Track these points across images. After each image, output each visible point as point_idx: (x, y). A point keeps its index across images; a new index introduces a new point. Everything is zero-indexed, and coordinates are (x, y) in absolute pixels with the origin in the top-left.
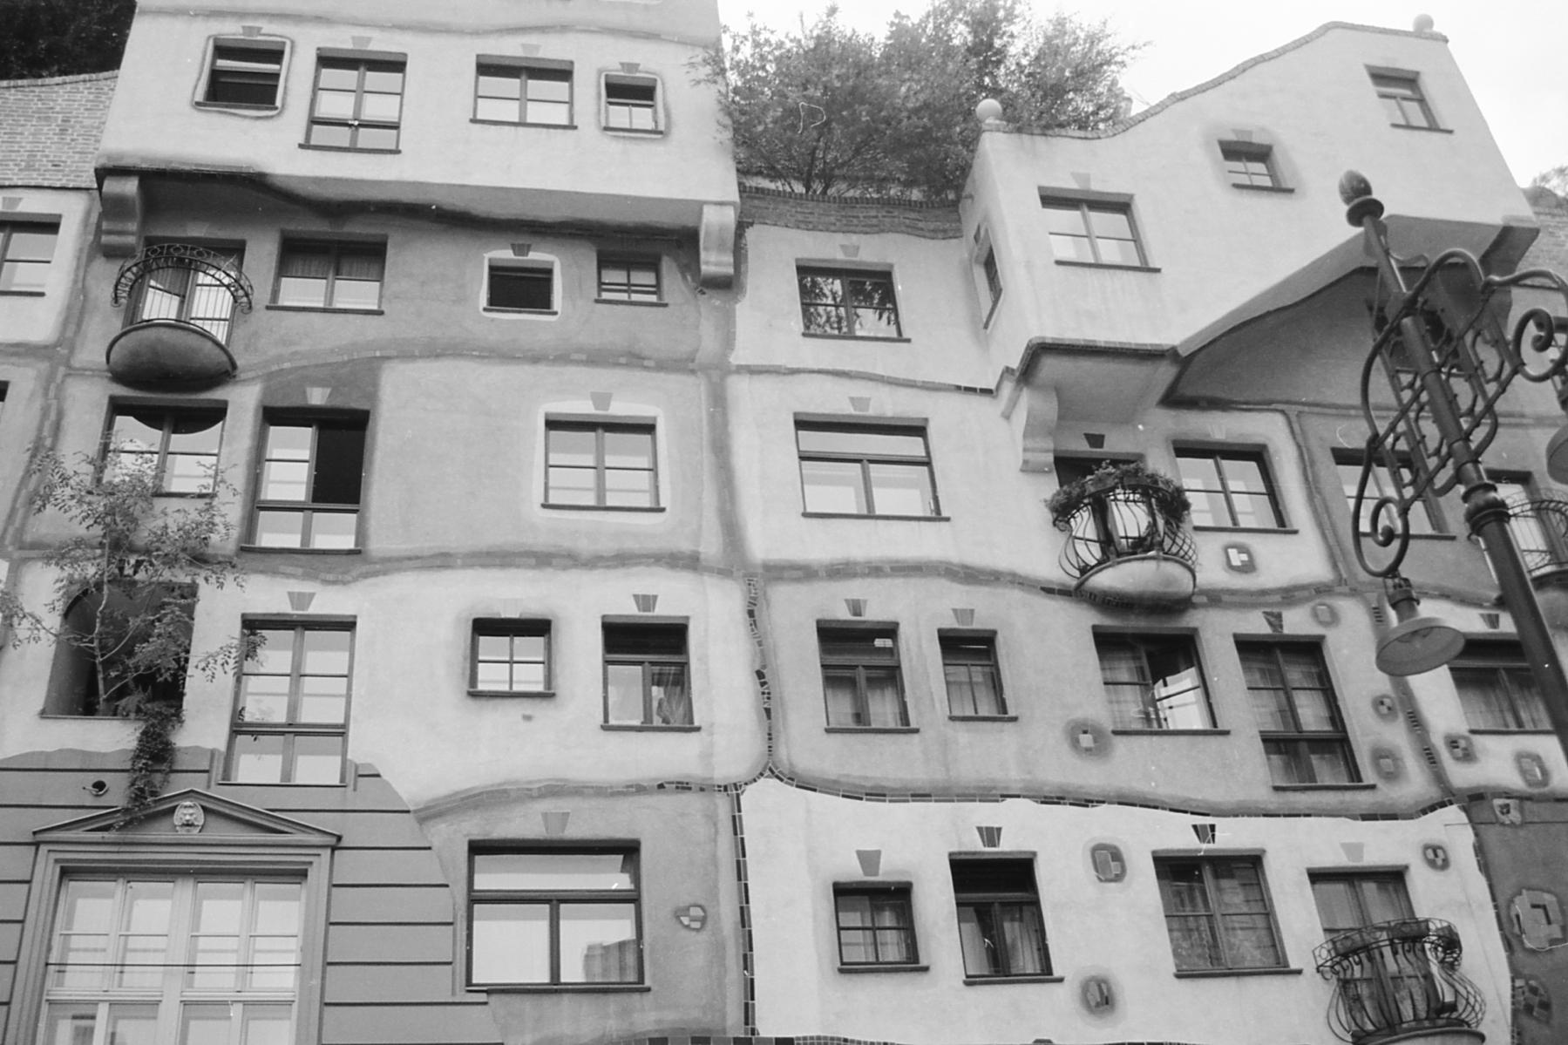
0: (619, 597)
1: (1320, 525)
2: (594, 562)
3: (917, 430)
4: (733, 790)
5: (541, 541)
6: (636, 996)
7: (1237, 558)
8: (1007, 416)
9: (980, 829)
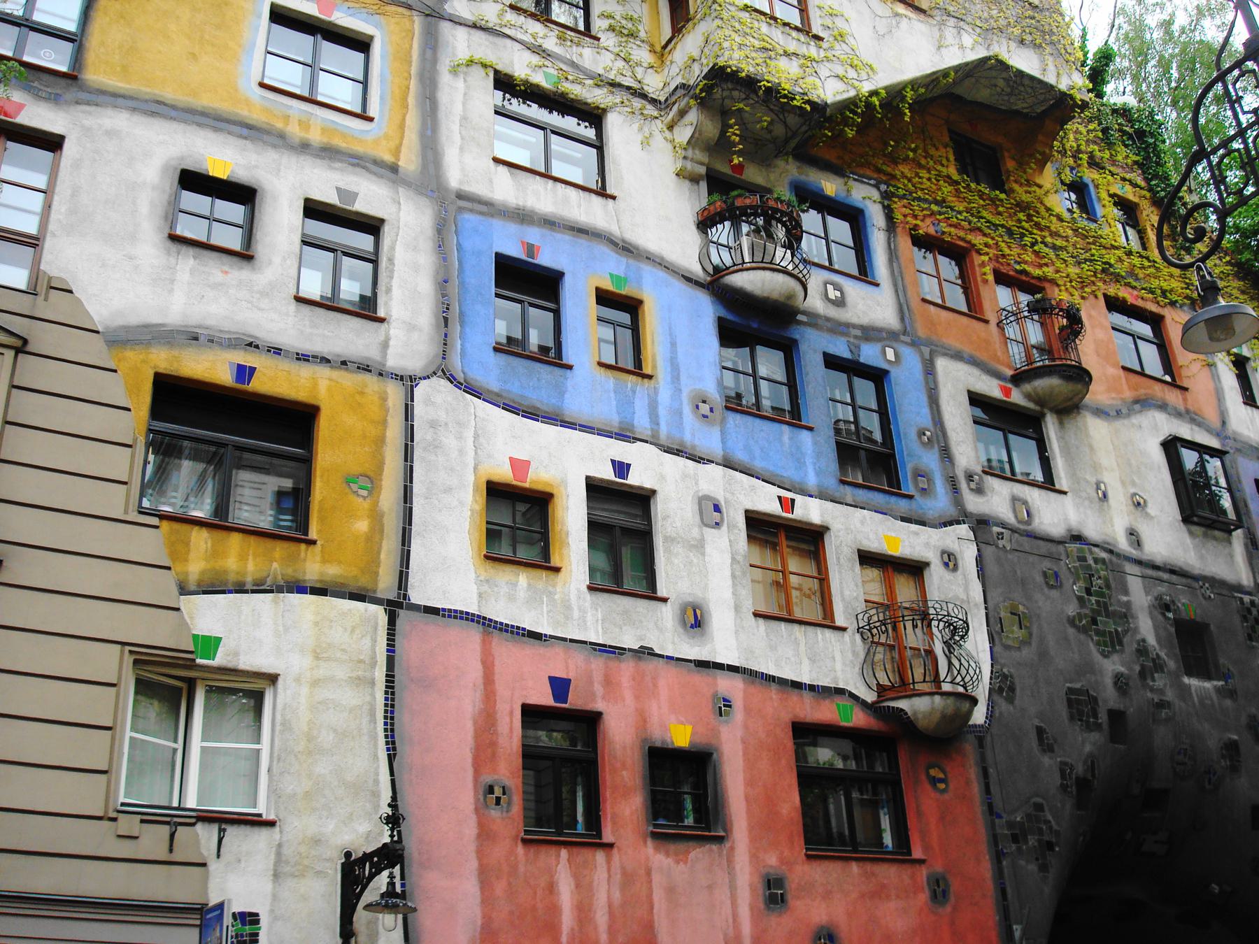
0: (326, 184)
1: (895, 285)
2: (304, 147)
3: (594, 117)
4: (409, 382)
5: (256, 116)
6: (303, 546)
7: (833, 294)
8: (671, 127)
9: (613, 462)
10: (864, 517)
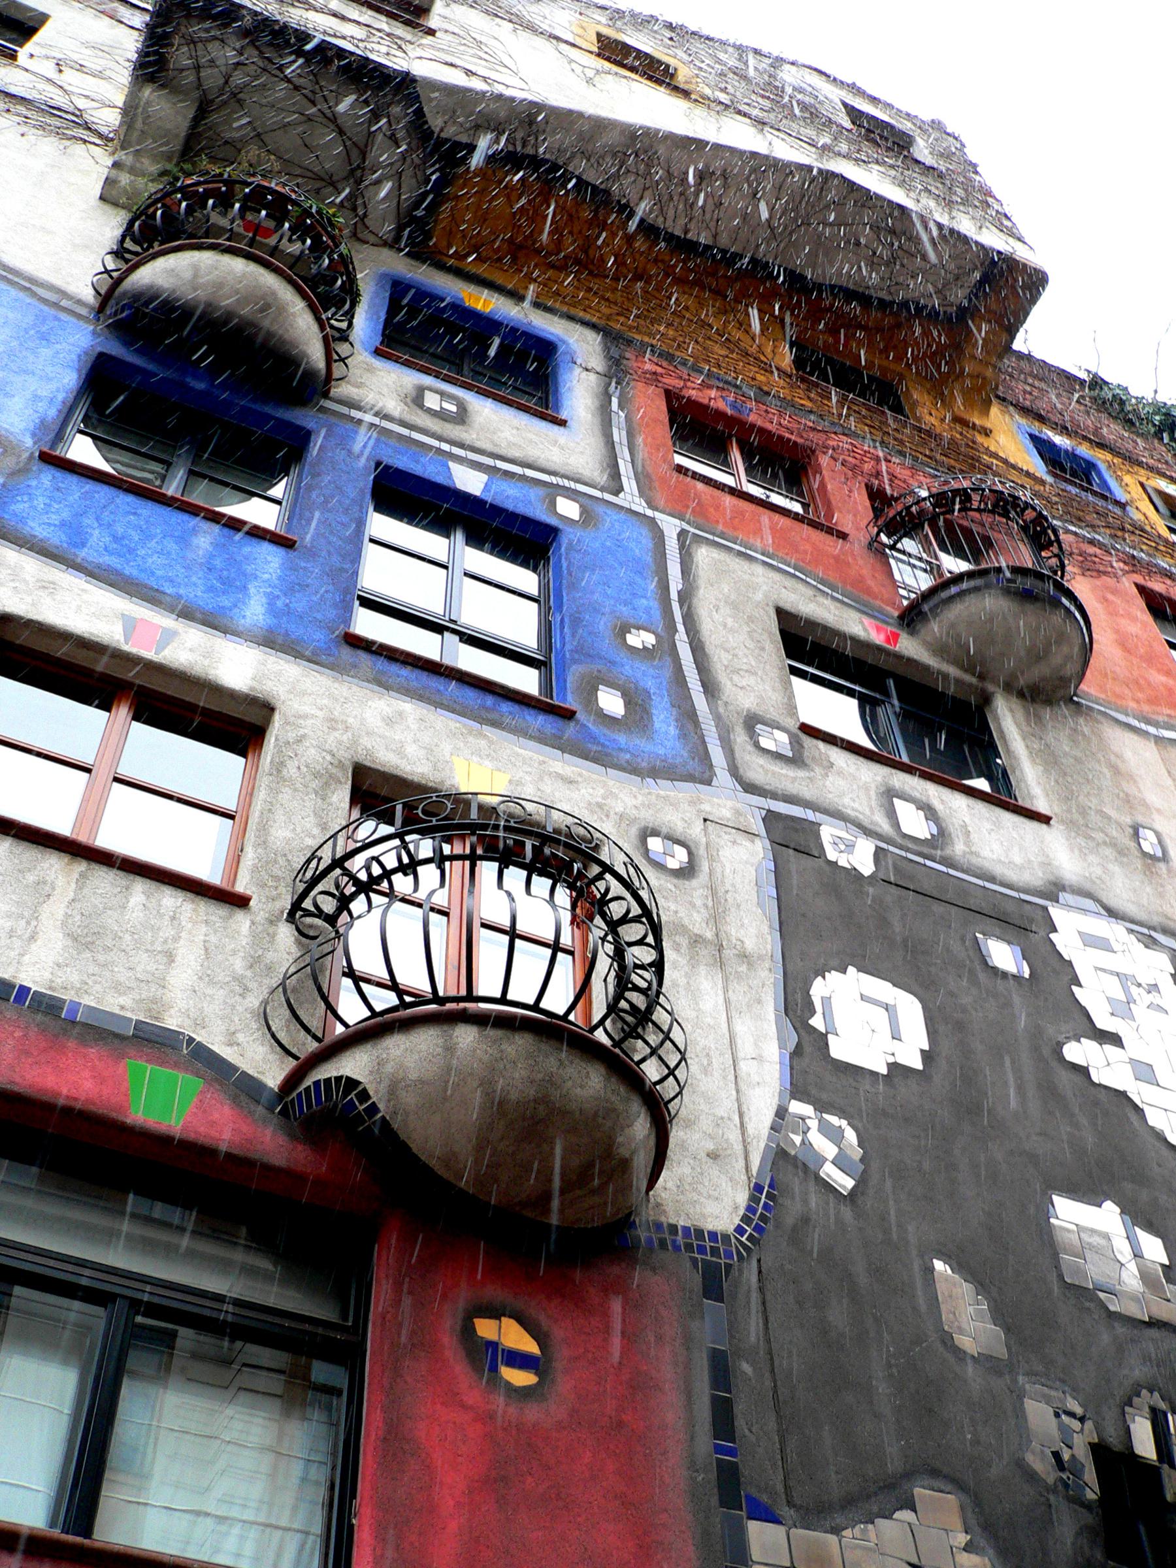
10: (401, 714)
